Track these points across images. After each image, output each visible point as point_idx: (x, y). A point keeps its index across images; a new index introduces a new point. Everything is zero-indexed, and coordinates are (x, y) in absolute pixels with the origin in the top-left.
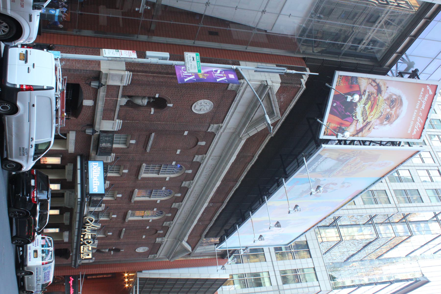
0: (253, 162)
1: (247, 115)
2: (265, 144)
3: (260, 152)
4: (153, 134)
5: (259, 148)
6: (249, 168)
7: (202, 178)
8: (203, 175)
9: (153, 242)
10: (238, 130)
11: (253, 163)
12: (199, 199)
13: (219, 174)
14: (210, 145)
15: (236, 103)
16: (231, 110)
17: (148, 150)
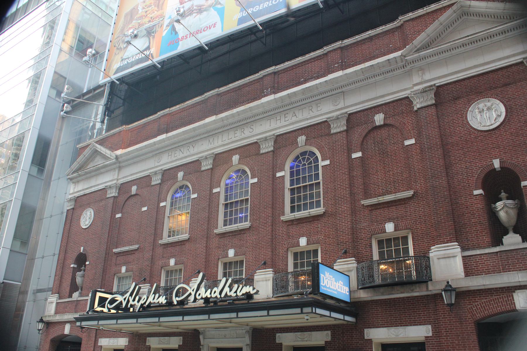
0: (167, 111)
1: (99, 171)
2: (139, 122)
3: (151, 117)
4: (114, 250)
5: (148, 122)
6: (178, 106)
7: (196, 150)
8: (188, 153)
9: (433, 110)
10: (114, 166)
11: (168, 109)
12: (245, 122)
13: (174, 138)
14: (137, 179)
15: (86, 191)
16: (93, 189)
17: (136, 247)
